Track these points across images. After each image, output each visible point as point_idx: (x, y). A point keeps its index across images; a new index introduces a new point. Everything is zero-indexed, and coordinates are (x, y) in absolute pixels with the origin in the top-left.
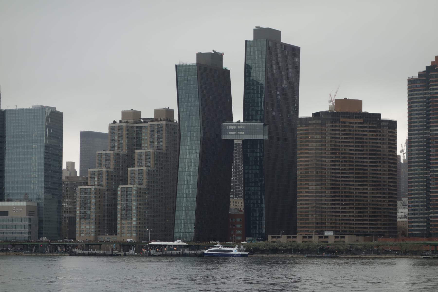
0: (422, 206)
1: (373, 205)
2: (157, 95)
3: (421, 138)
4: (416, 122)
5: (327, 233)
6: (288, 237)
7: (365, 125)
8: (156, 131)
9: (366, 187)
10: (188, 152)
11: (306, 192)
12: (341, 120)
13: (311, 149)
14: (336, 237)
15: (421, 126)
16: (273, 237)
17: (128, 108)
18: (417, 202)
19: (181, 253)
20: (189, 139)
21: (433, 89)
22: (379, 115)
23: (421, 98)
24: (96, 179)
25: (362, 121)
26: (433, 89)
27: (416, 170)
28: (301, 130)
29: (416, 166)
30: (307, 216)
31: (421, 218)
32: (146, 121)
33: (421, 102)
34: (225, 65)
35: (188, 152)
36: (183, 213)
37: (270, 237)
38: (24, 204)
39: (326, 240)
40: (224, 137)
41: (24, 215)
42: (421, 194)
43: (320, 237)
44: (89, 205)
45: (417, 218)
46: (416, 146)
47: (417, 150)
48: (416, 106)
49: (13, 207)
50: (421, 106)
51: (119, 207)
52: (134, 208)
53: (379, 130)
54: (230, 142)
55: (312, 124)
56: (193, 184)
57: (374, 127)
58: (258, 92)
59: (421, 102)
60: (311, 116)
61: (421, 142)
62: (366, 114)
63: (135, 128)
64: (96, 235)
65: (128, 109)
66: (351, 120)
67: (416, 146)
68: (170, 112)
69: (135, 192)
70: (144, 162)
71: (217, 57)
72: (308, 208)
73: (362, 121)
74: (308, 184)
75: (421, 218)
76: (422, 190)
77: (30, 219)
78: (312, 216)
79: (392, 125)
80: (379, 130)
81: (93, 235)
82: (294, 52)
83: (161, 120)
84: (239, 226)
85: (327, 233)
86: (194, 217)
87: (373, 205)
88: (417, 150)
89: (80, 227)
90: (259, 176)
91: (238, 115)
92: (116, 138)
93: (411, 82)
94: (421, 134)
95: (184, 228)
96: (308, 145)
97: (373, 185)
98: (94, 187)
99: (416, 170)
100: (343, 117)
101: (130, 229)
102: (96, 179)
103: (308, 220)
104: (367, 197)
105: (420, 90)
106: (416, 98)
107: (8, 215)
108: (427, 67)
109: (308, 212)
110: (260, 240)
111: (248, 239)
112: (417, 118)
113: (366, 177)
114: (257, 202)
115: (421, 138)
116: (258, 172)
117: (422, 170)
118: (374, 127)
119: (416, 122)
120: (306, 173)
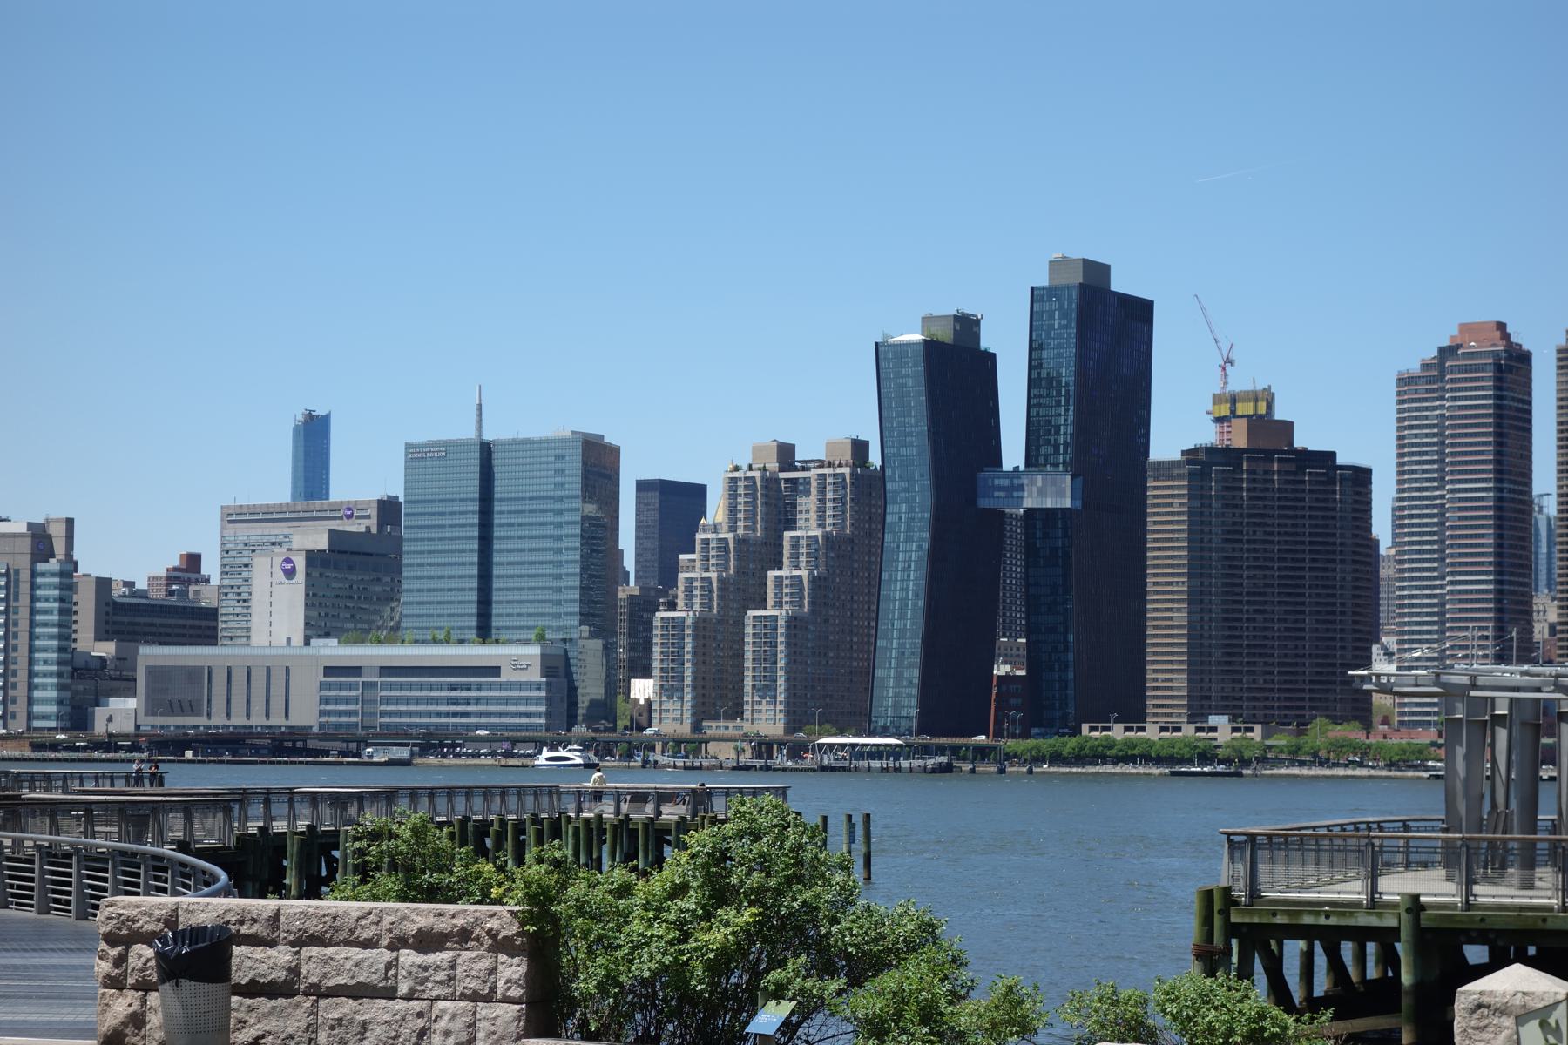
1: (1317, 656)
2: (837, 413)
5: (1213, 720)
6: (1127, 729)
14: (1235, 730)
21: (1455, 399)
26: (1455, 399)
28: (1156, 488)
34: (987, 342)
37: (1085, 728)
38: (535, 650)
39: (1211, 735)
40: (984, 503)
41: (535, 675)
43: (1199, 730)
54: (998, 516)
58: (1058, 403)
60: (1178, 457)
68: (860, 448)
71: (967, 325)
77: (549, 684)
79: (1361, 477)
82: (1141, 311)
83: (840, 465)
87: (1317, 656)
91: (1013, 453)
93: (1405, 381)
97: (1318, 613)
107: (498, 675)
108: (1441, 350)
111: (1035, 731)
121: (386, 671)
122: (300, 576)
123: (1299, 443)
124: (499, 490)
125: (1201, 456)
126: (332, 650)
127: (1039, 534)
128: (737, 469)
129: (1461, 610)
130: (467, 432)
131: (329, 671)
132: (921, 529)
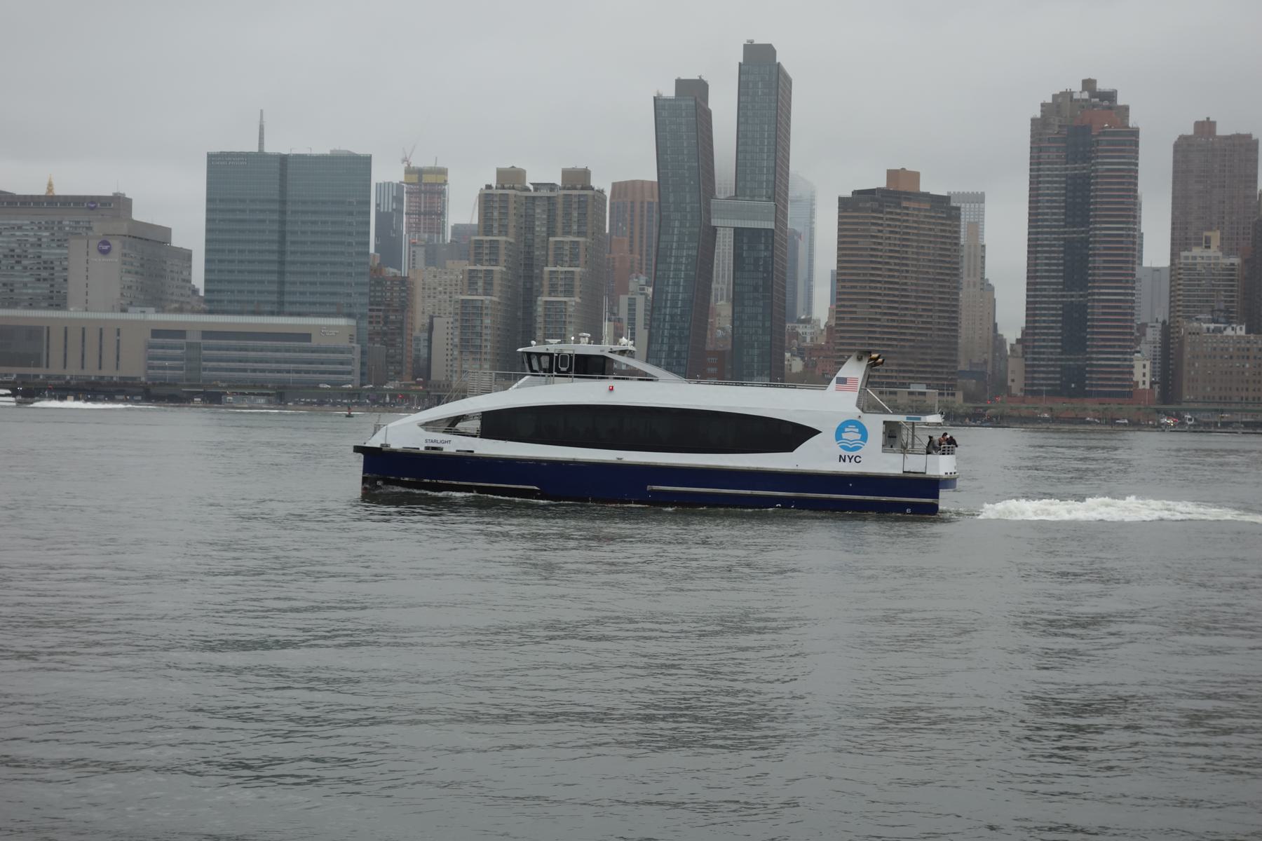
3: (1055, 239)
4: (1047, 214)
8: (575, 206)
10: (675, 245)
12: (905, 204)
13: (866, 249)
20: (677, 224)
24: (480, 283)
25: (928, 207)
27: (1045, 290)
32: (537, 186)
33: (1056, 182)
35: (675, 245)
36: (665, 347)
38: (342, 322)
47: (1047, 258)
49: (320, 327)
50: (1056, 189)
59: (1056, 182)
60: (849, 194)
61: (1054, 246)
62: (927, 195)
65: (507, 166)
69: (571, 309)
70: (567, 259)
76: (1053, 322)
85: (916, 388)
88: (1047, 258)
92: (496, 214)
94: (1054, 233)
96: (857, 243)
99: (1045, 290)
100: (906, 199)
102: (480, 283)
105: (1056, 163)
115: (1055, 239)
116: (761, 282)
117: (1054, 290)
119: (1047, 214)
120: (852, 287)
121: (207, 334)
122: (115, 258)
123: (923, 188)
126: (154, 317)
128: (488, 187)
129: (1104, 314)
130: (256, 150)
131: (156, 333)
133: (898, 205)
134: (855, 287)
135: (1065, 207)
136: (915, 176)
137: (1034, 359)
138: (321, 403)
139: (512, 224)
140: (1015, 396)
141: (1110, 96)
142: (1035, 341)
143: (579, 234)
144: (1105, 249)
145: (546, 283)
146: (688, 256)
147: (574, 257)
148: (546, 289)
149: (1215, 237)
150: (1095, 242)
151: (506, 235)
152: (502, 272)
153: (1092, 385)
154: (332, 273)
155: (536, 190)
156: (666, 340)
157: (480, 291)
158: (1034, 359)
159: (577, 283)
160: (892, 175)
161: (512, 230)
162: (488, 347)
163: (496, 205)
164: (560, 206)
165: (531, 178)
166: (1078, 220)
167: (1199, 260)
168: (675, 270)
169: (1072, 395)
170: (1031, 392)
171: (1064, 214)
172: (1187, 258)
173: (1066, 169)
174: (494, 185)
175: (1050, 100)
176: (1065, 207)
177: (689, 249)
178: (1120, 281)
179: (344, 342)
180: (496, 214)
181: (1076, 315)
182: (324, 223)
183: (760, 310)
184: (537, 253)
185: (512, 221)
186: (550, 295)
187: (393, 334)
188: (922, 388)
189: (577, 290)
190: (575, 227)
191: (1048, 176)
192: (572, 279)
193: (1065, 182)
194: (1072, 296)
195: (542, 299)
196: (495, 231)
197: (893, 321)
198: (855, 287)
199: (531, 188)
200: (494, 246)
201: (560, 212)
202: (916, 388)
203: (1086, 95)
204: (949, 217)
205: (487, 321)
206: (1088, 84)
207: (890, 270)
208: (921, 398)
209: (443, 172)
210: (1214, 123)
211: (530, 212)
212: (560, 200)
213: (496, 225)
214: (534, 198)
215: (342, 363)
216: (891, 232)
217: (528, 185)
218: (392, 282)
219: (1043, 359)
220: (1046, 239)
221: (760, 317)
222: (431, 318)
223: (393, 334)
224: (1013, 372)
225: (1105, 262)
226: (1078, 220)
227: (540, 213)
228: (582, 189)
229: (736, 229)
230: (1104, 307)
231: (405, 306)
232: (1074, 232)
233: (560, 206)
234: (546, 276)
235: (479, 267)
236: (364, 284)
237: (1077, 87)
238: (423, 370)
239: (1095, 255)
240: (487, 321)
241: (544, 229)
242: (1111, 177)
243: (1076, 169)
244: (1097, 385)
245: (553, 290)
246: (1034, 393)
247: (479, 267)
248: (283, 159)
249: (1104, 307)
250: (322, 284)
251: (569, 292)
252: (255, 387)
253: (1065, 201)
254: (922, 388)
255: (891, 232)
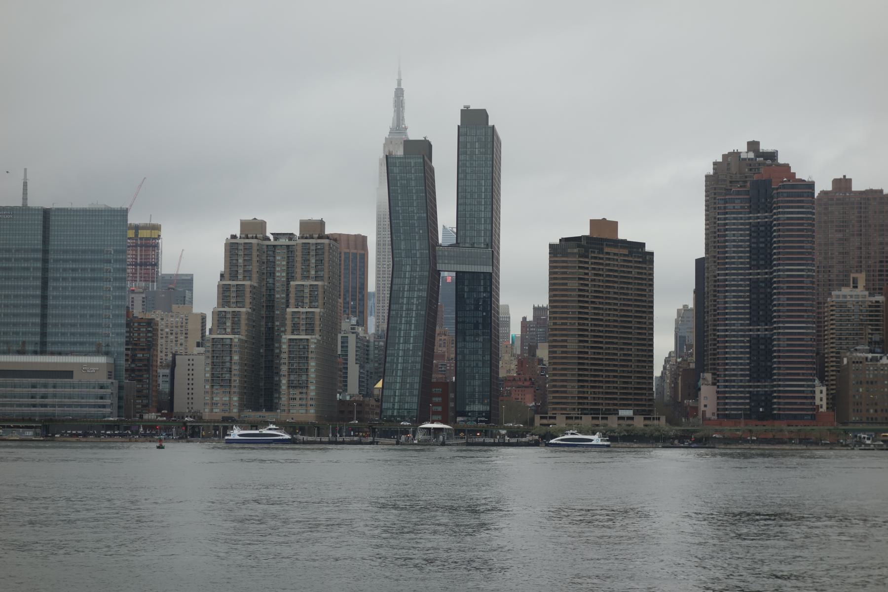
0: (742, 375)
3: (741, 280)
4: (734, 258)
7: (630, 259)
8: (313, 253)
9: (630, 347)
11: (563, 352)
12: (606, 250)
13: (574, 290)
15: (742, 263)
16: (542, 418)
17: (249, 217)
18: (734, 370)
19: (497, 441)
20: (408, 268)
22: (643, 245)
23: (742, 224)
24: (229, 324)
25: (626, 252)
29: (734, 319)
30: (565, 386)
31: (741, 392)
32: (277, 236)
33: (741, 230)
36: (399, 379)
38: (102, 360)
41: (104, 379)
42: (741, 358)
44: (228, 364)
45: (734, 392)
46: (734, 291)
47: (734, 297)
48: (734, 235)
49: (82, 364)
50: (741, 235)
51: (284, 369)
52: (313, 370)
53: (644, 266)
55: (573, 253)
56: (415, 337)
57: (640, 262)
58: (479, 204)
59: (741, 230)
60: (558, 242)
61: (741, 285)
63: (265, 247)
64: (240, 411)
66: (616, 251)
67: (734, 291)
69: (313, 346)
70: (307, 300)
72: (565, 375)
73: (626, 252)
74: (566, 341)
75: (741, 392)
76: (741, 353)
78: (573, 387)
80: (644, 266)
81: (235, 410)
84: (437, 399)
85: (623, 413)
86: (417, 386)
88: (734, 297)
89: (212, 398)
90: (480, 327)
92: (241, 261)
94: (741, 274)
95: (399, 402)
96: (566, 284)
97: (638, 345)
98: (237, 336)
101: (304, 402)
102: (229, 324)
103: (565, 392)
104: (631, 361)
105: (740, 213)
106: (734, 224)
107: (72, 377)
109: (566, 381)
110: (481, 421)
112: (734, 252)
113: (630, 333)
114: (477, 364)
115: (741, 280)
116: (480, 320)
117: (742, 325)
118: (640, 262)
120: (563, 324)
123: (621, 236)
124: (54, 243)
125: (583, 243)
127: (466, 289)
129: (788, 345)
130: (20, 204)
132: (420, 283)
133: (601, 251)
134: (565, 324)
135: (750, 252)
136: (614, 225)
137: (726, 387)
138: (85, 435)
139: (255, 270)
140: (710, 419)
141: (772, 156)
142: (726, 370)
143: (317, 278)
144: (788, 288)
145: (289, 322)
146: (419, 297)
147: (313, 299)
148: (289, 328)
149: (862, 278)
150: (779, 282)
151: (250, 280)
152: (248, 313)
153: (779, 409)
154: (92, 316)
155: (276, 239)
156: (399, 373)
157: (228, 330)
158: (726, 387)
159: (317, 322)
160: (593, 223)
161: (255, 276)
162: (236, 381)
163: (241, 253)
164: (299, 253)
165: (271, 230)
166: (762, 262)
167: (849, 298)
168: (408, 310)
169: (762, 418)
170: (723, 415)
171: (750, 257)
172: (838, 296)
173: (750, 218)
174: (238, 236)
175: (720, 160)
176: (750, 252)
177: (419, 290)
178: (802, 317)
179: (104, 379)
180: (241, 261)
181: (762, 347)
182: (83, 270)
183: (480, 345)
184: (277, 296)
185: (254, 267)
186: (293, 333)
187: (139, 370)
188: (629, 413)
189: (317, 329)
190: (313, 272)
191: (734, 224)
192: (312, 319)
193: (749, 230)
194: (758, 330)
195: (286, 337)
196: (240, 277)
197: (599, 353)
198: (565, 324)
199: (272, 237)
200: (240, 289)
201: (299, 259)
202: (623, 413)
203: (751, 155)
204: (644, 262)
205: (236, 358)
206: (753, 145)
207: (595, 308)
208: (629, 422)
209: (157, 228)
210: (850, 180)
211: (271, 259)
212: (299, 248)
213: (241, 271)
214: (274, 246)
215: (101, 398)
216: (596, 275)
217: (268, 234)
218: (139, 323)
219: (734, 387)
220: (734, 280)
221: (480, 352)
222: (174, 356)
223: (139, 370)
224: (706, 398)
225: (788, 299)
226: (762, 262)
227: (281, 261)
228: (320, 237)
229: (457, 273)
230: (788, 340)
231: (151, 345)
232: (758, 274)
233: (299, 253)
234: (289, 317)
235: (227, 309)
236: (120, 325)
237: (743, 148)
238: (167, 404)
239: (779, 293)
240: (236, 358)
241: (284, 274)
242: (792, 225)
243: (758, 218)
244: (784, 409)
245: (295, 329)
246: (727, 416)
247: (227, 309)
248: (46, 213)
249: (788, 340)
250: (81, 325)
251: (310, 330)
252: (23, 420)
253: (750, 246)
254: (629, 413)
255: (596, 275)
